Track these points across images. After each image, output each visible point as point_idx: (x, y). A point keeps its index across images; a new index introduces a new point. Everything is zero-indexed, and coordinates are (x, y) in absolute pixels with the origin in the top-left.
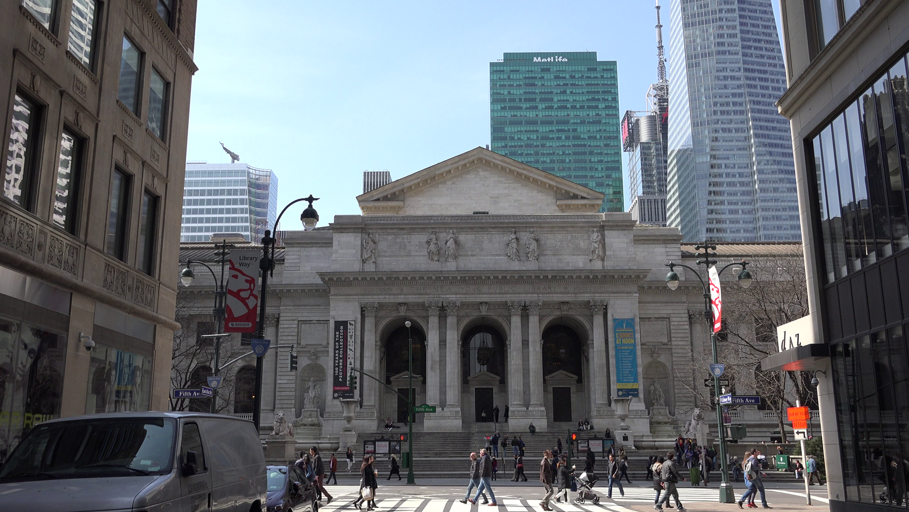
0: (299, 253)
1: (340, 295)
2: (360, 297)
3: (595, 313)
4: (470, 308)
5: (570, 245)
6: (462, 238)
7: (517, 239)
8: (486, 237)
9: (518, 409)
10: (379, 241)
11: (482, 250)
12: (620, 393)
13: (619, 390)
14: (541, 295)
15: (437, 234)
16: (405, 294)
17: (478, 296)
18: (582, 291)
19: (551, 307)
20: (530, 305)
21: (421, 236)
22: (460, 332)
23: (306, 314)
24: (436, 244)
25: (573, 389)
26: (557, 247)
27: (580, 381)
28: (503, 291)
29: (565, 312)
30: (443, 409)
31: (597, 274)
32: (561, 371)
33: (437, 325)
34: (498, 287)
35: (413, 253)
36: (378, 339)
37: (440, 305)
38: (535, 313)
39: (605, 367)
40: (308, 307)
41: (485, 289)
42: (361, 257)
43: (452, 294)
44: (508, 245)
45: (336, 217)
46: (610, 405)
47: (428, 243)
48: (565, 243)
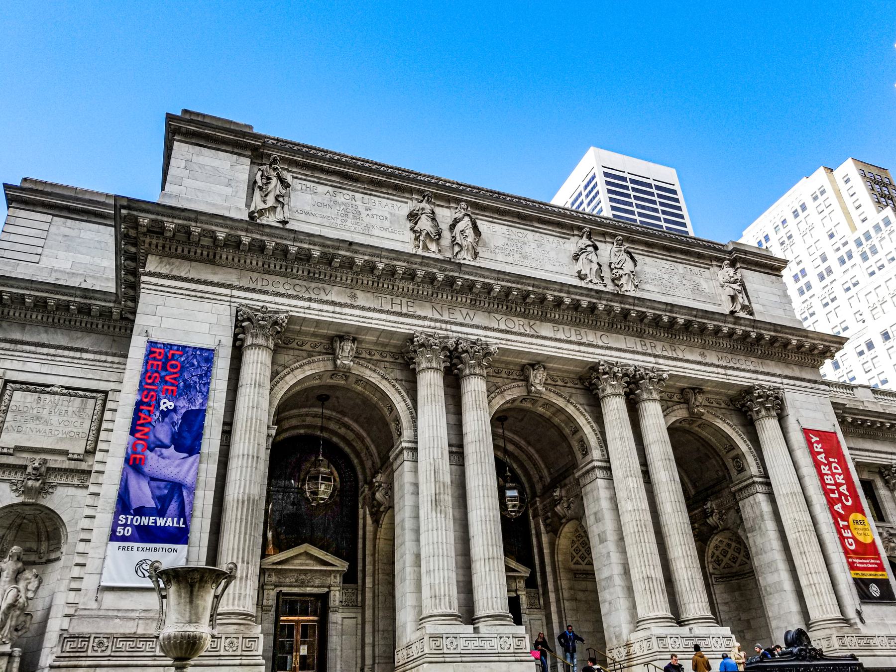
0: (45, 226)
1: (175, 278)
2: (236, 293)
3: (763, 413)
4: (503, 375)
5: (685, 282)
6: (482, 225)
14: (661, 361)
17: (534, 340)
21: (395, 203)
23: (36, 367)
26: (664, 281)
28: (584, 340)
30: (476, 630)
31: (763, 332)
34: (573, 332)
35: (376, 232)
37: (451, 343)
40: (45, 350)
41: (546, 330)
42: (248, 205)
43: (477, 327)
44: (576, 257)
45: (185, 111)
47: (413, 217)
48: (675, 277)
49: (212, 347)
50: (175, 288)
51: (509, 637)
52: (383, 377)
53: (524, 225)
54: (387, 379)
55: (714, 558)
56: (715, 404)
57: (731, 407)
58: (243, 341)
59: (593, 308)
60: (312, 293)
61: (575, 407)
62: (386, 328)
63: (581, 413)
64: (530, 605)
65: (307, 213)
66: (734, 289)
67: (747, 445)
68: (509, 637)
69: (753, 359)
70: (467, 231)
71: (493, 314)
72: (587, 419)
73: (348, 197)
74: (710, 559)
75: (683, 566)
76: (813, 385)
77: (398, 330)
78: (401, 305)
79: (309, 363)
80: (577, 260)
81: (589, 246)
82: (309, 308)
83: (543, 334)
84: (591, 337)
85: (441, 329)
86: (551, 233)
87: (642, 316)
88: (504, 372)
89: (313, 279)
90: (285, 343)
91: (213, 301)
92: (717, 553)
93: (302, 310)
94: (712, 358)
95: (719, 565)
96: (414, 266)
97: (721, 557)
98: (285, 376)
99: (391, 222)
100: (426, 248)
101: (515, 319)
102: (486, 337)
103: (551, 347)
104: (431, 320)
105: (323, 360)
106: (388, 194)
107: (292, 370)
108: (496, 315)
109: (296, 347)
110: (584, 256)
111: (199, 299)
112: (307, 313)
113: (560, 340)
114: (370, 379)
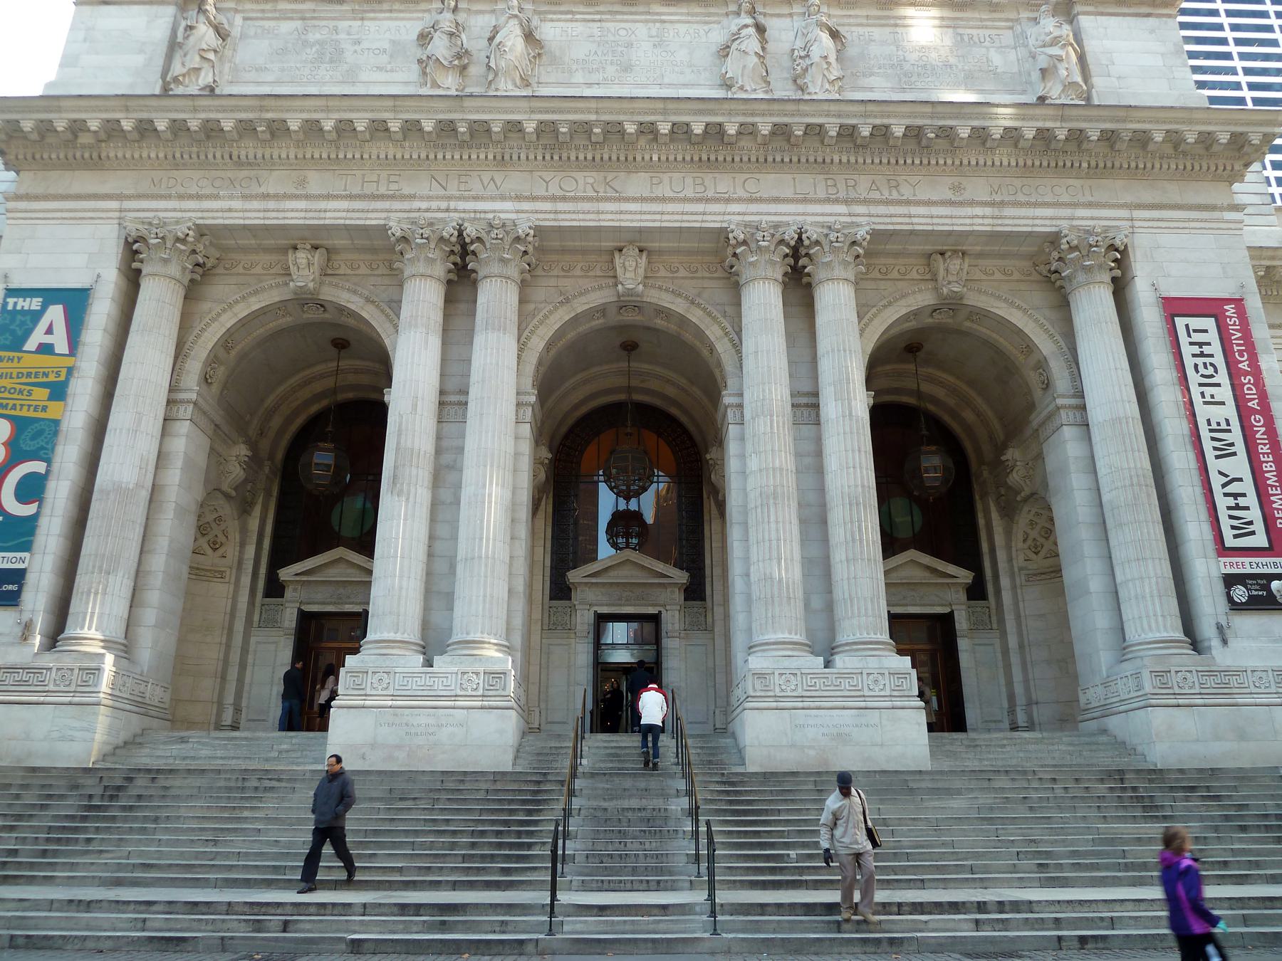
3: (1081, 277)
6: (550, 31)
7: (761, 29)
8: (641, 30)
9: (787, 663)
10: (243, 36)
11: (627, 68)
12: (1240, 593)
13: (1230, 581)
15: (461, 17)
16: (307, 197)
18: (1022, 198)
19: (895, 274)
20: (817, 243)
22: (532, 359)
24: (451, 35)
25: (961, 623)
27: (976, 591)
28: (710, 194)
29: (953, 277)
32: (912, 554)
33: (437, 316)
34: (689, 181)
35: (364, 76)
36: (192, 378)
37: (449, 231)
38: (839, 272)
39: (1151, 481)
41: (637, 184)
42: (164, 76)
43: (503, 198)
44: (724, 51)
46: (1195, 644)
47: (424, 38)
49: (87, 286)
50: (44, 211)
51: (477, 674)
52: (368, 300)
53: (632, 13)
54: (373, 302)
55: (1029, 542)
56: (998, 276)
57: (1035, 277)
58: (139, 271)
59: (715, 133)
60: (238, 186)
61: (704, 310)
62: (348, 222)
63: (714, 319)
64: (690, 624)
65: (259, 69)
66: (1051, 56)
67: (1056, 342)
68: (477, 674)
69: (1071, 181)
70: (509, 44)
71: (539, 173)
72: (723, 329)
73: (325, 31)
74: (1021, 545)
75: (844, 558)
76: (1205, 215)
77: (368, 222)
78: (378, 182)
79: (256, 292)
80: (727, 55)
81: (746, 26)
82: (230, 210)
83: (631, 192)
84: (723, 183)
85: (439, 210)
86: (683, 18)
87: (816, 131)
88: (579, 267)
89: (240, 164)
90: (226, 269)
91: (96, 222)
92: (1033, 534)
93: (220, 214)
94: (978, 188)
95: (1036, 553)
96: (385, 115)
97: (1041, 540)
98: (219, 315)
99: (391, 56)
100: (435, 85)
101: (579, 176)
102: (517, 212)
103: (641, 213)
104: (422, 198)
105: (278, 285)
106: (391, 11)
107: (230, 306)
108: (544, 174)
109: (241, 271)
110: (735, 46)
111: (79, 222)
112: (226, 218)
113: (663, 200)
114: (349, 305)
